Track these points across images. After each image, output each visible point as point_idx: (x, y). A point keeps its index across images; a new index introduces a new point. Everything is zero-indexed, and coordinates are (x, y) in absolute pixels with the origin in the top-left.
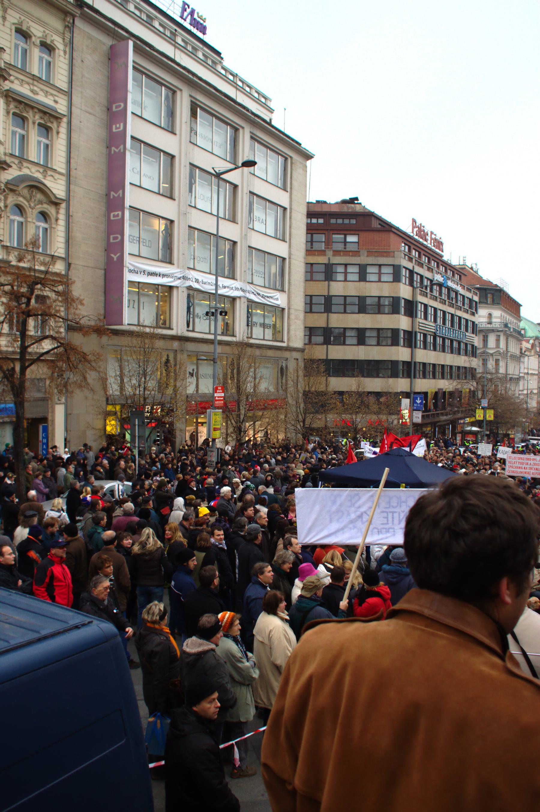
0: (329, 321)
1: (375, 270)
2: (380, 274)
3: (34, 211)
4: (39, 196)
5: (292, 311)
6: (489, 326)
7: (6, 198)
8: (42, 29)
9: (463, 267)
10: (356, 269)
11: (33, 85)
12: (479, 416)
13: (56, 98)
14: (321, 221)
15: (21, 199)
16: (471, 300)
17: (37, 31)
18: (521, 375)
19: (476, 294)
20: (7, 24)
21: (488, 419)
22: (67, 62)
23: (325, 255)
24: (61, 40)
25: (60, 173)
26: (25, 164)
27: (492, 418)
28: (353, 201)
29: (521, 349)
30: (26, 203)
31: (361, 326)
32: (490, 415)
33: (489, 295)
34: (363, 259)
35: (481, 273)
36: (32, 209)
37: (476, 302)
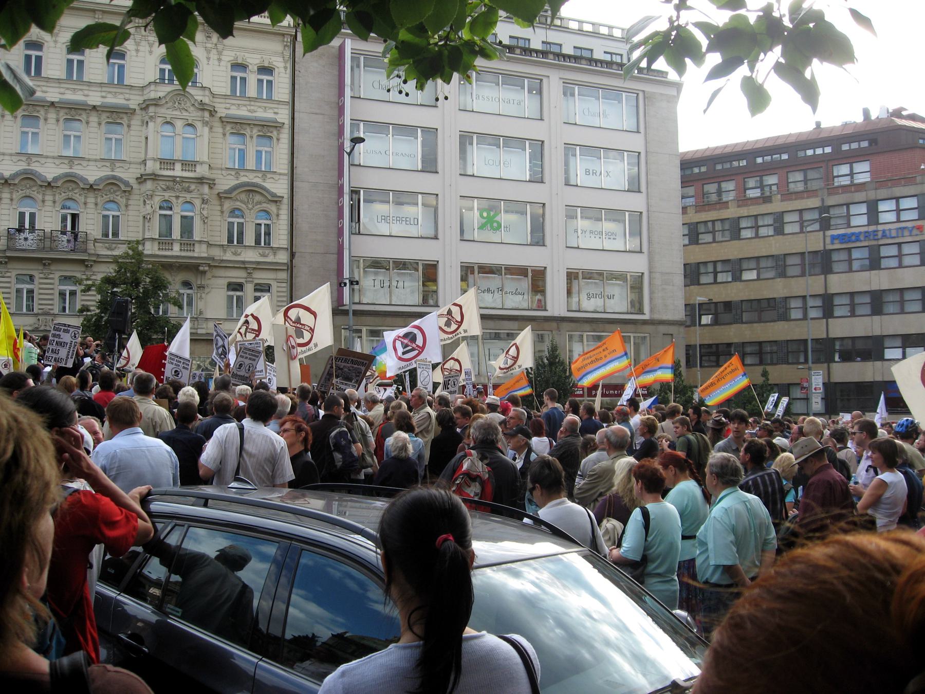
0: (828, 286)
1: (890, 205)
2: (898, 211)
3: (252, 211)
4: (258, 198)
7: (221, 205)
8: (259, 56)
10: (863, 209)
11: (250, 105)
13: (276, 110)
14: (828, 150)
15: (238, 203)
17: (254, 61)
20: (222, 63)
22: (288, 76)
23: (817, 196)
24: (281, 59)
25: (280, 174)
26: (242, 174)
28: (897, 113)
30: (244, 206)
31: (875, 287)
34: (872, 195)
36: (250, 210)
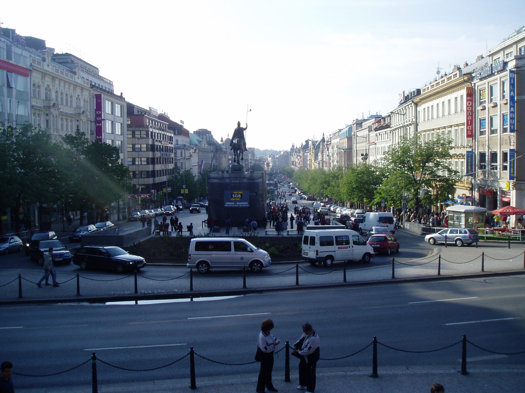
1: (139, 133)
5: (125, 159)
6: (177, 146)
9: (162, 115)
12: (182, 192)
16: (170, 137)
18: (191, 167)
19: (172, 133)
21: (186, 193)
27: (187, 193)
29: (190, 154)
31: (134, 157)
32: (187, 191)
33: (176, 130)
34: (134, 129)
35: (171, 119)
37: (172, 137)
